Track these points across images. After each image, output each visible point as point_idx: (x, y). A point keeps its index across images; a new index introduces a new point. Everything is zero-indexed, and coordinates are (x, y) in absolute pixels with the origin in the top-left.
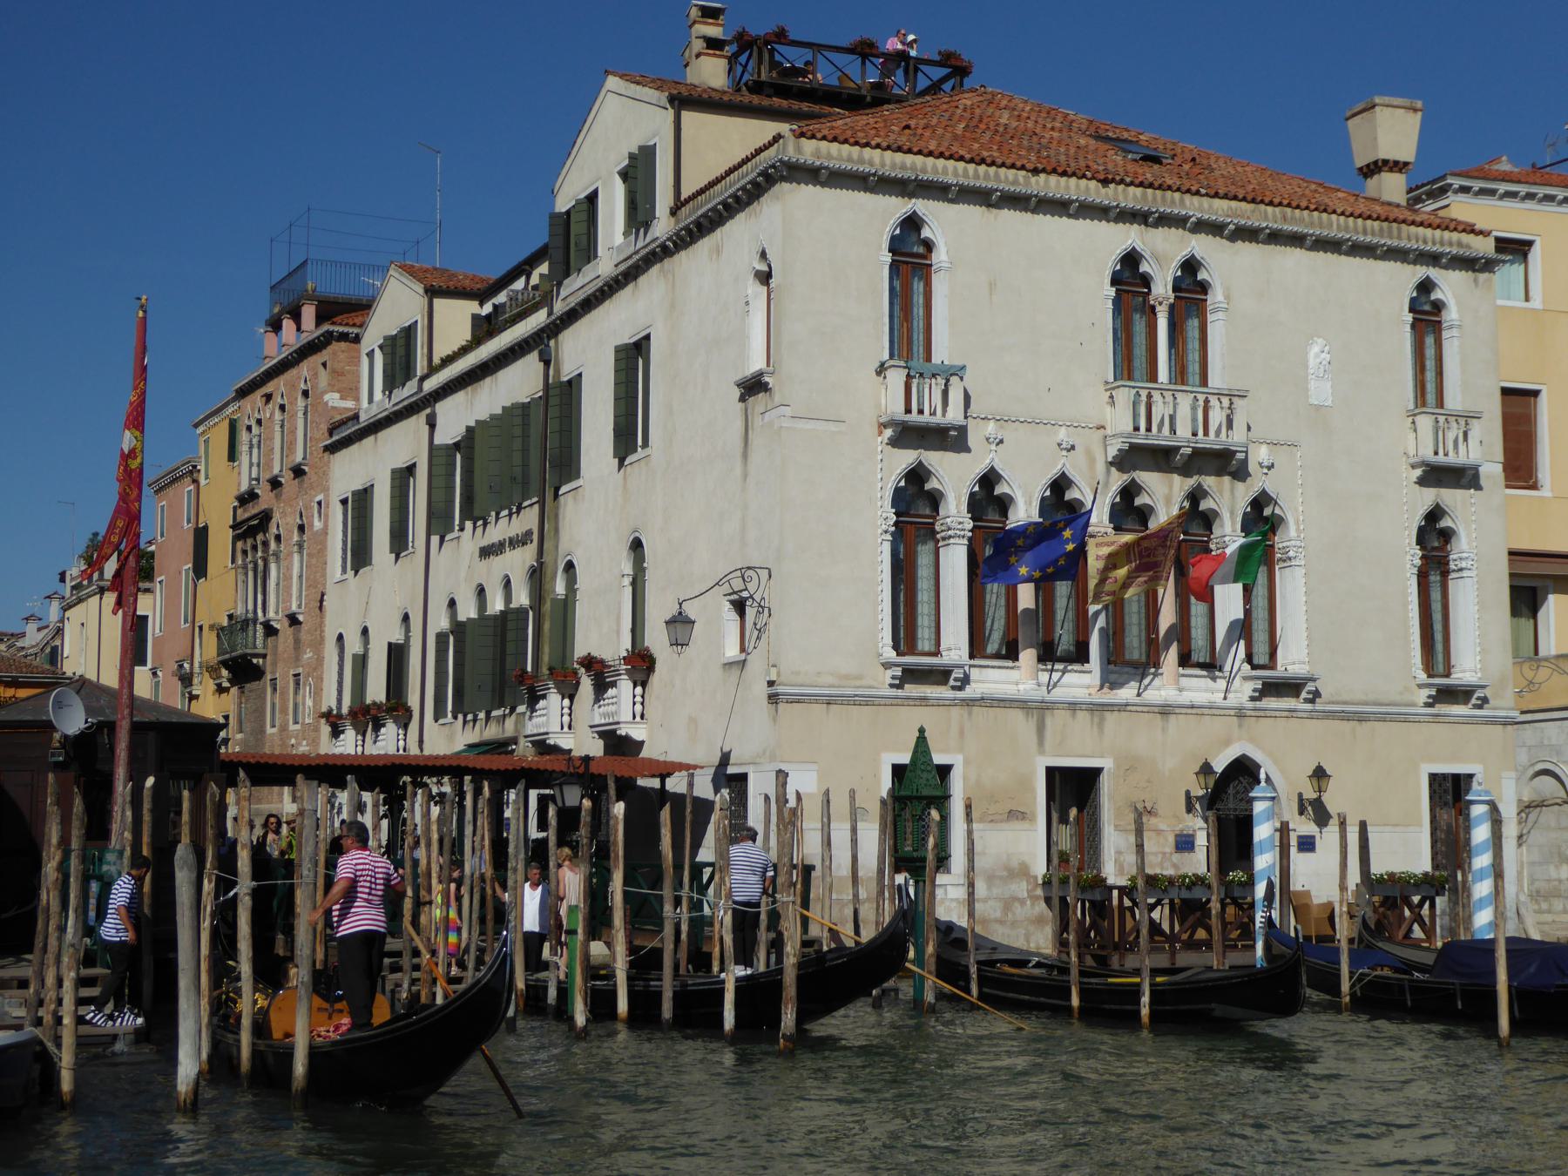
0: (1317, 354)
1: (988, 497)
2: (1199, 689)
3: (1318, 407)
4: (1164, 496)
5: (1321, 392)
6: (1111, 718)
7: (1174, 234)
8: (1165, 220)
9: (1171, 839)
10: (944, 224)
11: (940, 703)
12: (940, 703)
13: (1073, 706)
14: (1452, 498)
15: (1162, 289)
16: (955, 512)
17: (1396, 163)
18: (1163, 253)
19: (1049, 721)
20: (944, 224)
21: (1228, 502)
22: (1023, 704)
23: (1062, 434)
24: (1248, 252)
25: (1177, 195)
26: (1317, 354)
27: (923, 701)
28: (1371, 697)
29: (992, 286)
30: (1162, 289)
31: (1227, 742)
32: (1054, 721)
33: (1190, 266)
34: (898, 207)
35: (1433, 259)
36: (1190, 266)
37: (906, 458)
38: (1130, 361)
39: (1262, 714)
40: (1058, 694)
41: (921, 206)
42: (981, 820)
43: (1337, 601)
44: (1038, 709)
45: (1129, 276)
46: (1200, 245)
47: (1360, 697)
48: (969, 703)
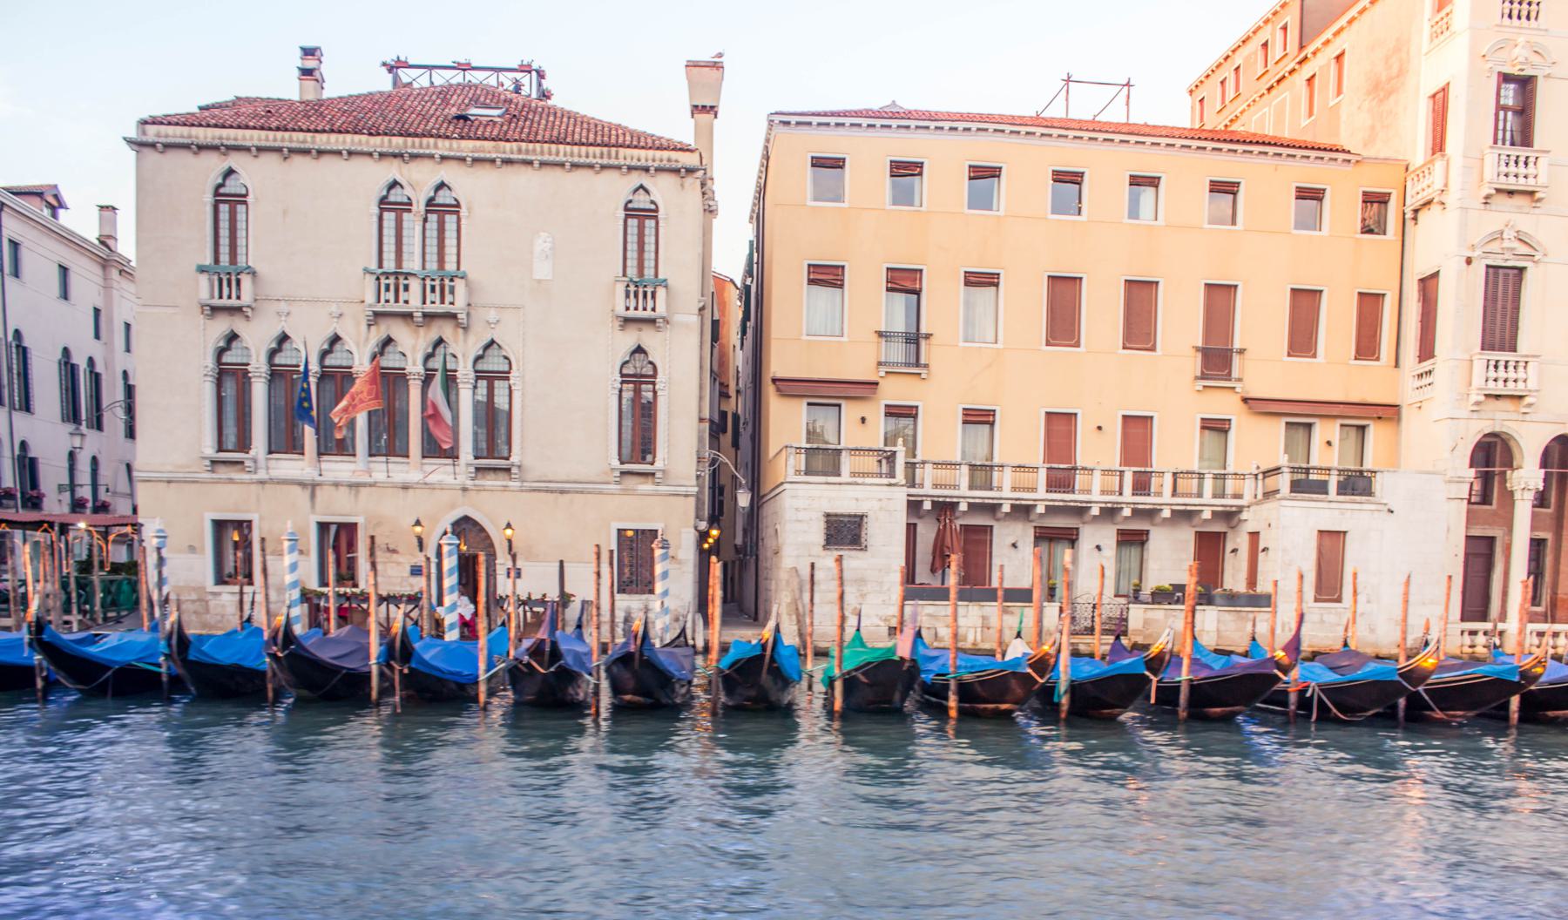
0: (542, 244)
2: (440, 471)
3: (539, 281)
4: (411, 348)
5: (542, 270)
6: (363, 491)
7: (428, 164)
9: (408, 569)
13: (336, 485)
18: (419, 180)
20: (253, 174)
21: (463, 351)
22: (302, 484)
23: (334, 308)
24: (486, 175)
25: (432, 140)
26: (542, 244)
27: (231, 481)
28: (573, 478)
29: (285, 213)
31: (453, 506)
34: (213, 165)
39: (480, 489)
40: (329, 476)
41: (235, 160)
42: (272, 553)
44: (312, 487)
46: (448, 173)
47: (564, 478)
48: (262, 482)
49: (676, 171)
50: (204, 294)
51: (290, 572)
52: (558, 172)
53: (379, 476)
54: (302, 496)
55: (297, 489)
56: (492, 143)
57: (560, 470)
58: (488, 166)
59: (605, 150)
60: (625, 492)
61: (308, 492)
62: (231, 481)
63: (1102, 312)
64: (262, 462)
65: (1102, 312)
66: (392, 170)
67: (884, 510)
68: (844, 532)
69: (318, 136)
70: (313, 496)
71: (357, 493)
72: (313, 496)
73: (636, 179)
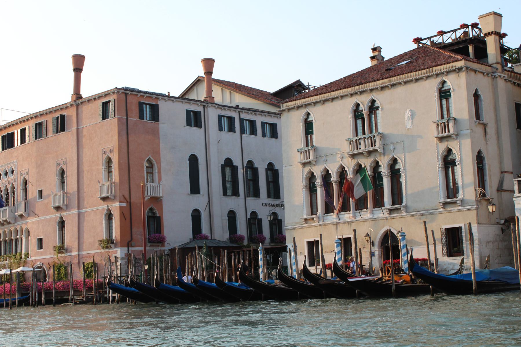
8: (362, 92)
11: (315, 226)
12: (315, 226)
13: (344, 223)
16: (318, 181)
17: (489, 33)
18: (364, 101)
19: (338, 227)
22: (332, 224)
24: (387, 93)
26: (408, 114)
31: (383, 227)
32: (340, 227)
37: (307, 169)
41: (309, 110)
42: (325, 253)
48: (321, 225)
49: (454, 71)
50: (299, 160)
51: (331, 255)
53: (358, 218)
54: (333, 227)
55: (332, 226)
56: (388, 79)
58: (387, 88)
59: (428, 70)
60: (446, 212)
61: (335, 227)
62: (312, 226)
64: (321, 218)
69: (332, 93)
70: (337, 228)
71: (351, 225)
72: (337, 228)
73: (439, 79)
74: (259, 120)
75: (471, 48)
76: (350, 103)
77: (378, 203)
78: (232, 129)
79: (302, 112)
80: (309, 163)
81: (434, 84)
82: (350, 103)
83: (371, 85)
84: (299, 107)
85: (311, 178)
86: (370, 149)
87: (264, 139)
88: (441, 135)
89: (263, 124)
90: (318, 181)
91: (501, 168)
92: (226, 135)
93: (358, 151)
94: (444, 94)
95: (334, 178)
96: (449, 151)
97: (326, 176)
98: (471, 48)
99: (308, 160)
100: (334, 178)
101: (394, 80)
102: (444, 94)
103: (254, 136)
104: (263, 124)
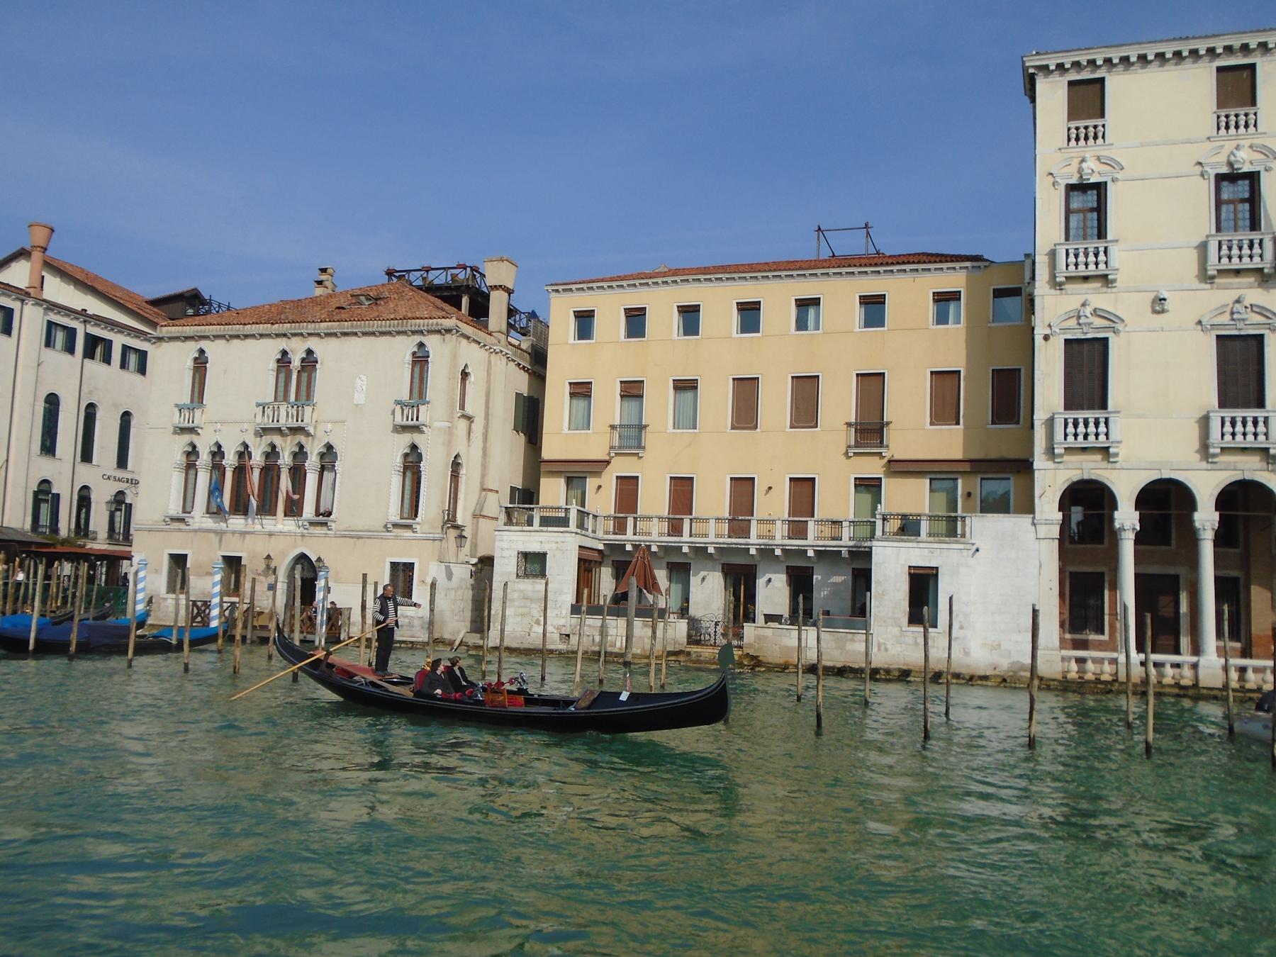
0: (362, 382)
1: (218, 453)
2: (289, 525)
5: (359, 398)
6: (248, 536)
10: (214, 350)
13: (234, 532)
14: (418, 439)
15: (296, 363)
16: (204, 458)
18: (297, 350)
20: (214, 350)
22: (215, 532)
27: (180, 530)
29: (225, 371)
30: (296, 363)
31: (295, 547)
33: (310, 352)
35: (421, 332)
36: (310, 352)
38: (281, 393)
41: (204, 344)
43: (365, 487)
45: (284, 360)
46: (313, 343)
47: (360, 528)
49: (439, 332)
52: (372, 338)
54: (214, 539)
55: (212, 535)
57: (360, 523)
62: (180, 530)
63: (775, 402)
65: (775, 402)
66: (282, 344)
67: (563, 551)
68: (534, 563)
73: (418, 339)
74: (118, 341)
75: (465, 301)
76: (273, 348)
77: (294, 509)
78: (70, 349)
79: (191, 349)
80: (192, 430)
81: (407, 345)
82: (273, 348)
83: (311, 328)
84: (187, 338)
85: (192, 452)
86: (295, 424)
87: (123, 372)
88: (405, 423)
89: (126, 349)
90: (204, 458)
91: (482, 483)
92: (56, 357)
93: (275, 425)
94: (420, 360)
95: (230, 460)
96: (414, 447)
97: (218, 453)
98: (465, 301)
99: (191, 425)
100: (230, 460)
101: (346, 326)
102: (420, 360)
103: (105, 366)
104: (126, 349)
